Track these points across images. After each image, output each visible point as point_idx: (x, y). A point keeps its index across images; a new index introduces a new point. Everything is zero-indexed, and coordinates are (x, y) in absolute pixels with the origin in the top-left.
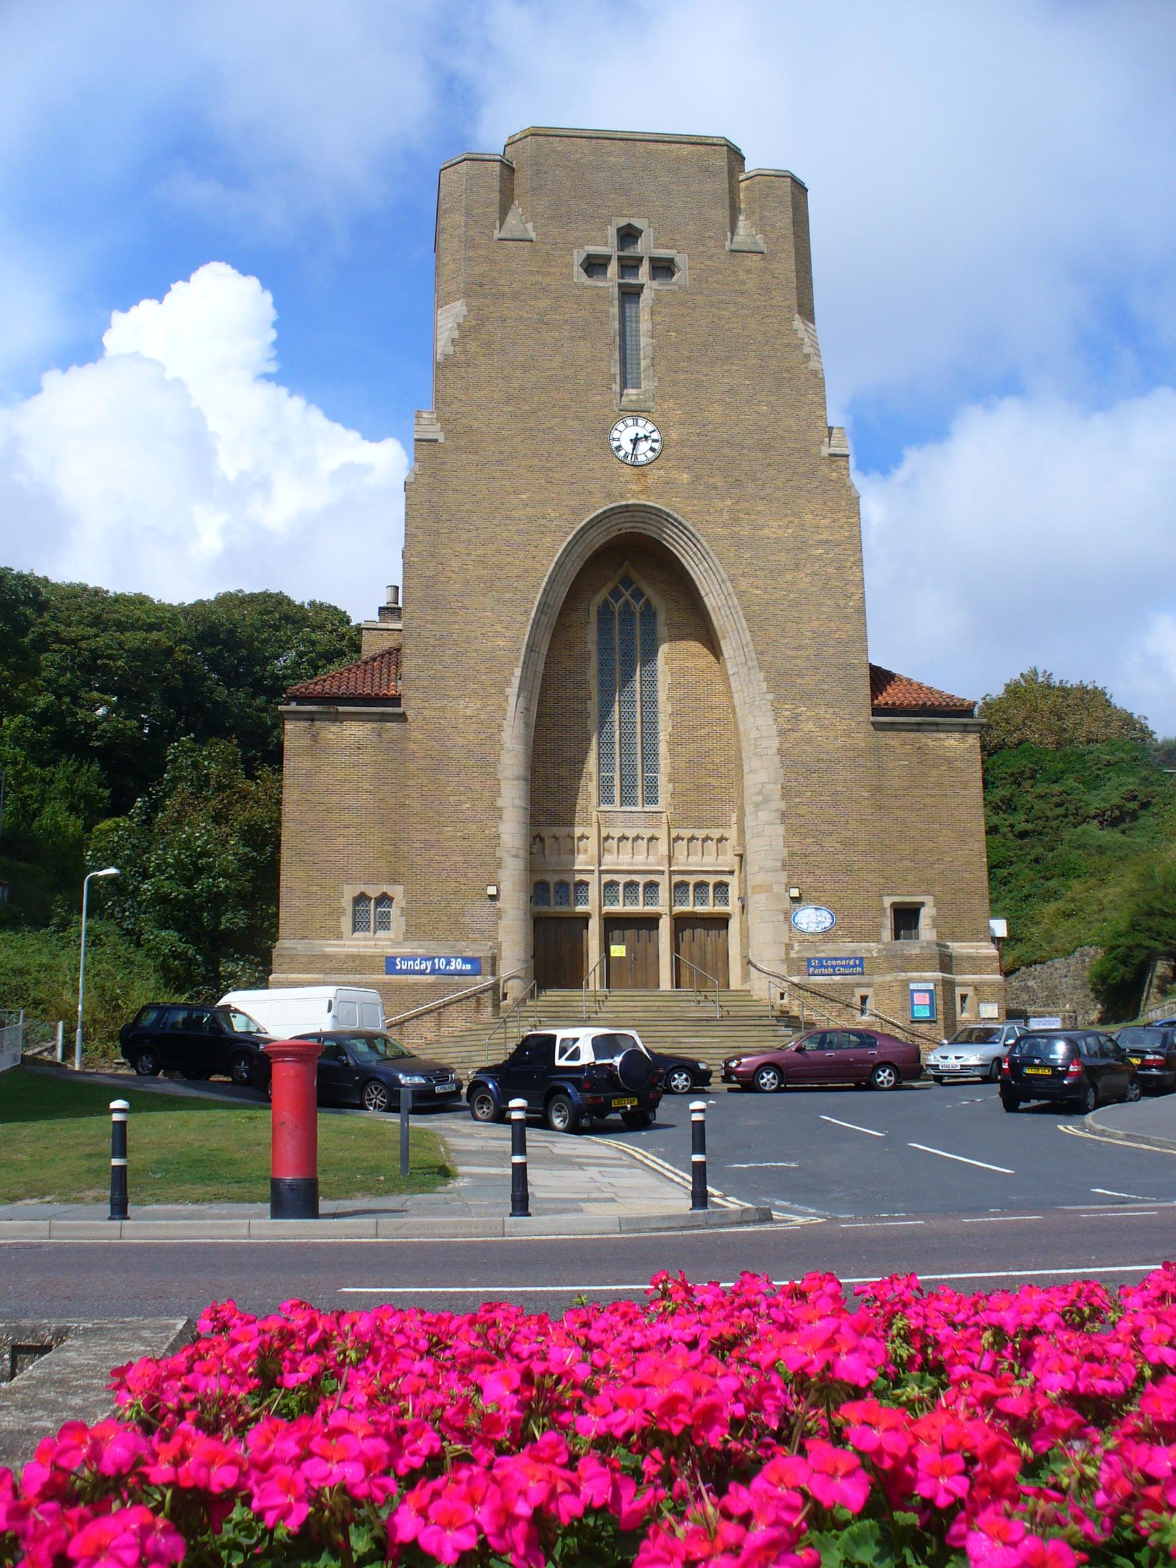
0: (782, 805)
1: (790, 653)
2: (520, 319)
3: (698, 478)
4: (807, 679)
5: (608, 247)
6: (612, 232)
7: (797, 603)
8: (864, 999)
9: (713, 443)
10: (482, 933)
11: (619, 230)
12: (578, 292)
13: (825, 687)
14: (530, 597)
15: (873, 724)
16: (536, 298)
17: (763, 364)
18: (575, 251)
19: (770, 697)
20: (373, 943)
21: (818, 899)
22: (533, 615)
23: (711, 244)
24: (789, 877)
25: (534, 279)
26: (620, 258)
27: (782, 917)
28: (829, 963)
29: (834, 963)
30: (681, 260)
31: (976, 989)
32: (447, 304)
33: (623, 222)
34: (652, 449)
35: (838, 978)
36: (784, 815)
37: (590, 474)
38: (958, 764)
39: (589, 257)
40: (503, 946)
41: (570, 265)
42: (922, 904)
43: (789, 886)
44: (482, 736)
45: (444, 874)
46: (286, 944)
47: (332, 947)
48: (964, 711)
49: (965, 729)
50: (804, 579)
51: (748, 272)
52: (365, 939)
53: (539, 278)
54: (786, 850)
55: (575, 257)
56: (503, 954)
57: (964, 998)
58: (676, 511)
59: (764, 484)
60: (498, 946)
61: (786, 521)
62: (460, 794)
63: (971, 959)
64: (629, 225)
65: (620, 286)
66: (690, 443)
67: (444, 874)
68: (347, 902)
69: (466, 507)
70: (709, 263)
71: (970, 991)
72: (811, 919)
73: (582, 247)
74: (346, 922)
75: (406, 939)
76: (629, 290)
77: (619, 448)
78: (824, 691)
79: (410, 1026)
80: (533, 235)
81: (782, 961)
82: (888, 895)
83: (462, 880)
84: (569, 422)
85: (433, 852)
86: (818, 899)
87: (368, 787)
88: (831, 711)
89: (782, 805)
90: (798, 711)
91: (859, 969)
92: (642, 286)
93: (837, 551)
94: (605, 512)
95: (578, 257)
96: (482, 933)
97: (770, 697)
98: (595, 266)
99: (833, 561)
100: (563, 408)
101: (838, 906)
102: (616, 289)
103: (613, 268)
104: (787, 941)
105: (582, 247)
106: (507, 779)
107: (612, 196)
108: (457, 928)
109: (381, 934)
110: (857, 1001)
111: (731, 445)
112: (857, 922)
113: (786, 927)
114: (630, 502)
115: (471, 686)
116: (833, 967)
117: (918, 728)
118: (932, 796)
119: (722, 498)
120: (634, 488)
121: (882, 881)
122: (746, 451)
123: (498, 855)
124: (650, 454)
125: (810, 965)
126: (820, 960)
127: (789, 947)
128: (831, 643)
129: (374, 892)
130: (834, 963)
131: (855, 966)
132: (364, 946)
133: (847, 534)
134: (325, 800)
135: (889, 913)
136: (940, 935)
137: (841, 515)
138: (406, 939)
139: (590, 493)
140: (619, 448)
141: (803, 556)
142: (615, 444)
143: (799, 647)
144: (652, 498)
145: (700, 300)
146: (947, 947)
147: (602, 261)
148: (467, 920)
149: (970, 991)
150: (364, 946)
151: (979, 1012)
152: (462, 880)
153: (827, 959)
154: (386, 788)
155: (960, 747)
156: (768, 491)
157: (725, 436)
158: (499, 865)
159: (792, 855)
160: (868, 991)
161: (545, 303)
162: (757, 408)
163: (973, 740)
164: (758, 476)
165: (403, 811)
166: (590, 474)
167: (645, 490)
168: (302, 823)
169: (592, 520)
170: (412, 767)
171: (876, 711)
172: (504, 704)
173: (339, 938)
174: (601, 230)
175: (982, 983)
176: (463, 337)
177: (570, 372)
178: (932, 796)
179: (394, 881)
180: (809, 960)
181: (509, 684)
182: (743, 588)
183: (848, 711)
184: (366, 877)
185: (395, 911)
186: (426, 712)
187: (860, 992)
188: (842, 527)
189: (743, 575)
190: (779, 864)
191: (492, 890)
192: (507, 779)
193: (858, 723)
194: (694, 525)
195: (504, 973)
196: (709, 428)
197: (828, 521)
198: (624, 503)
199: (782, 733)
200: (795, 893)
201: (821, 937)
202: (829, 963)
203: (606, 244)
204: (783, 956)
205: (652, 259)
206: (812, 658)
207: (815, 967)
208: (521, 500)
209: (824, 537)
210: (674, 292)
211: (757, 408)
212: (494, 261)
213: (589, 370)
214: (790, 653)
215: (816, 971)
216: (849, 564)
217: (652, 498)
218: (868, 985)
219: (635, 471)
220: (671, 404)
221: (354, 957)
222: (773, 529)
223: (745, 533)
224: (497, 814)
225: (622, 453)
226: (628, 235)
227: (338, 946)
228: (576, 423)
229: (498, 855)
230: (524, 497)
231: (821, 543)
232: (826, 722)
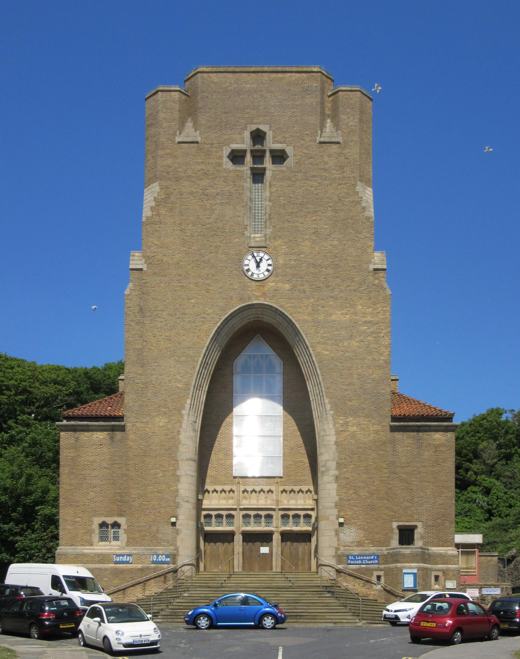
0: (336, 473)
1: (345, 387)
2: (192, 193)
3: (294, 287)
4: (354, 402)
5: (245, 143)
6: (247, 135)
7: (350, 358)
8: (379, 577)
9: (304, 265)
10: (168, 542)
11: (251, 133)
12: (226, 175)
13: (365, 406)
14: (196, 359)
15: (391, 427)
16: (201, 180)
17: (337, 215)
18: (224, 148)
19: (332, 412)
20: (110, 547)
21: (355, 523)
22: (197, 369)
23: (308, 139)
24: (339, 511)
25: (199, 167)
26: (252, 151)
27: (334, 533)
28: (359, 558)
29: (362, 558)
30: (289, 151)
31: (444, 573)
32: (149, 185)
33: (254, 127)
34: (268, 270)
35: (362, 566)
36: (337, 478)
37: (232, 287)
38: (441, 448)
39: (233, 151)
40: (180, 549)
41: (220, 158)
42: (416, 527)
43: (338, 517)
44: (168, 437)
45: (148, 511)
46: (61, 549)
47: (87, 550)
48: (449, 418)
49: (446, 429)
50: (354, 344)
51: (330, 156)
52: (105, 545)
53: (203, 167)
54: (337, 497)
55: (224, 151)
56: (180, 553)
57: (437, 578)
58: (281, 307)
59: (334, 288)
60: (177, 549)
61: (345, 311)
62: (157, 469)
63: (441, 555)
64: (258, 130)
65: (252, 169)
66: (290, 266)
67: (148, 511)
68: (95, 526)
69: (160, 308)
70: (306, 151)
71: (440, 574)
72: (350, 535)
73: (228, 145)
74: (96, 537)
75: (127, 545)
76: (256, 172)
77: (248, 270)
78: (364, 409)
79: (129, 591)
80: (199, 139)
81: (334, 557)
82: (396, 521)
83: (158, 514)
84: (219, 256)
85: (141, 500)
86: (355, 523)
87: (106, 465)
88: (367, 419)
89: (336, 473)
90: (348, 420)
91: (376, 561)
92: (265, 169)
93: (375, 327)
94: (239, 309)
95: (226, 151)
96: (168, 542)
97: (332, 412)
98: (237, 157)
99: (372, 333)
100: (216, 247)
101: (366, 527)
102: (249, 172)
103: (248, 158)
104: (336, 546)
105: (228, 145)
106: (183, 460)
107: (247, 111)
108: (155, 540)
109: (114, 543)
110: (374, 579)
111: (314, 266)
112: (377, 536)
113: (336, 539)
114: (254, 302)
115: (163, 409)
116: (362, 560)
117: (418, 429)
118: (424, 467)
119: (308, 298)
120: (257, 294)
121: (392, 513)
122: (324, 269)
123: (177, 501)
124: (266, 273)
125: (348, 559)
126: (354, 556)
127: (337, 549)
128: (369, 381)
129: (110, 520)
130: (362, 558)
131: (374, 559)
132: (104, 549)
133: (382, 317)
134: (83, 472)
135: (397, 531)
136: (425, 543)
137: (379, 306)
138: (127, 545)
139: (231, 298)
140: (248, 270)
141: (355, 331)
142: (246, 268)
143: (350, 384)
144: (267, 300)
145: (299, 175)
146: (428, 550)
147: (241, 154)
148: (160, 536)
149: (440, 574)
150: (104, 549)
151: (445, 585)
152: (158, 514)
153: (358, 556)
154: (116, 466)
155: (444, 440)
156: (336, 293)
157: (312, 261)
158: (177, 506)
159: (341, 499)
160: (381, 573)
161: (205, 183)
162: (331, 243)
163: (451, 436)
164: (330, 284)
165: (125, 478)
166: (232, 287)
167: (264, 295)
168: (70, 485)
169: (232, 314)
170: (131, 454)
171: (394, 419)
172: (181, 419)
173: (92, 545)
174: (240, 133)
175: (448, 570)
176: (158, 206)
177: (220, 225)
178: (424, 467)
179: (120, 515)
180: (348, 556)
181: (183, 408)
182: (319, 351)
183: (377, 419)
184: (105, 513)
185: (121, 531)
186: (137, 424)
187: (376, 573)
188: (379, 313)
189: (318, 343)
190: (333, 505)
191: (173, 520)
192: (183, 460)
193: (383, 426)
194: (291, 314)
195: (180, 563)
196: (302, 256)
197: (370, 309)
198: (250, 303)
199: (338, 433)
200: (341, 520)
201: (356, 544)
202: (359, 558)
203: (243, 143)
204: (334, 554)
205: (271, 151)
206: (358, 390)
207: (351, 560)
208: (191, 303)
209: (369, 318)
210: (283, 172)
211: (331, 243)
212: (176, 157)
213: (232, 223)
214: (345, 387)
215: (352, 562)
216: (382, 335)
217: (267, 300)
218: (381, 570)
219: (258, 283)
220: (280, 242)
221: (99, 555)
222: (338, 316)
223: (321, 317)
224: (177, 479)
225: (250, 273)
226: (258, 136)
227: (90, 549)
228: (223, 256)
229: (177, 501)
230: (193, 301)
231: (365, 322)
232: (364, 426)
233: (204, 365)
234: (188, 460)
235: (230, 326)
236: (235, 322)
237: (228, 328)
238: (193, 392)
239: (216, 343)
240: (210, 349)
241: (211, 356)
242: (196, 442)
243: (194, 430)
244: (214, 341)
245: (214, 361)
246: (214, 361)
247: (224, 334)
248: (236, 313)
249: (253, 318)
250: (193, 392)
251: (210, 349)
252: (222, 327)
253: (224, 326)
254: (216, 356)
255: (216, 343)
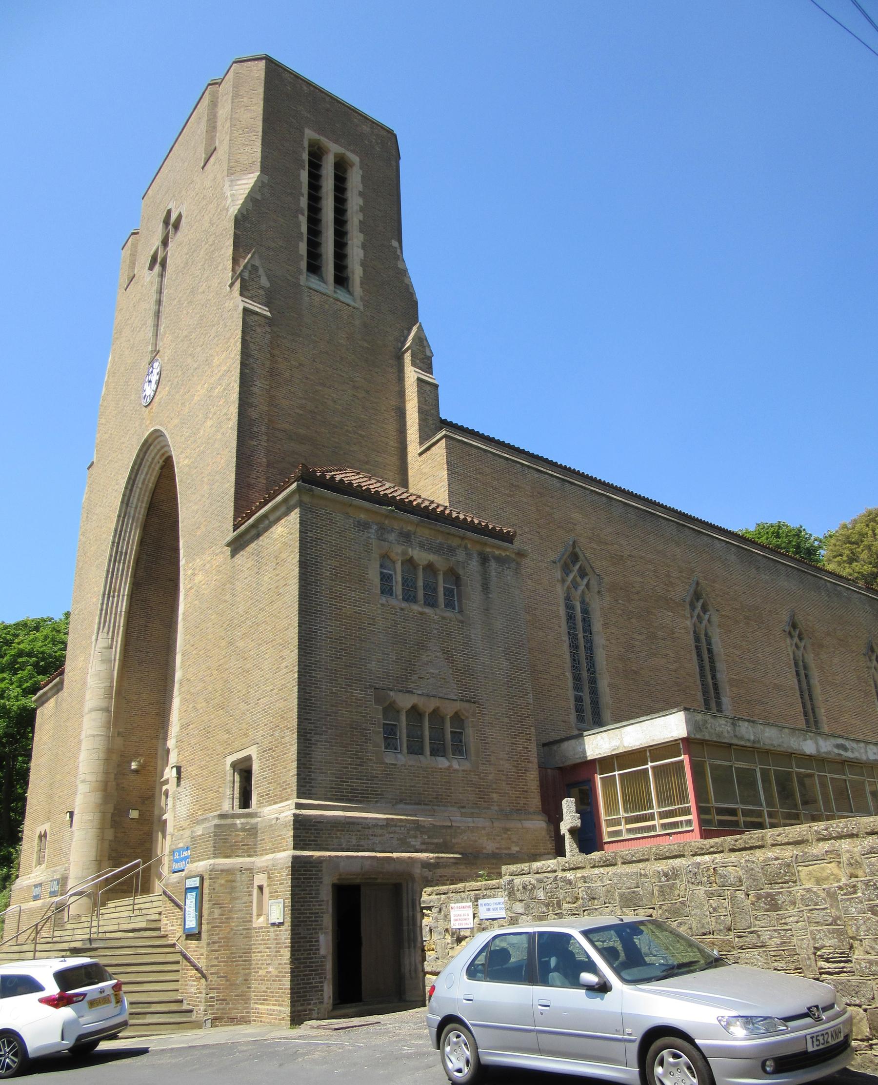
233: (116, 557)
234: (91, 710)
235: (140, 485)
236: (143, 476)
237: (138, 490)
238: (102, 604)
239: (128, 519)
240: (121, 531)
241: (124, 540)
242: (113, 678)
243: (108, 661)
244: (124, 518)
245: (132, 546)
246: (132, 546)
247: (135, 501)
248: (138, 462)
249: (161, 458)
250: (102, 604)
251: (121, 531)
252: (128, 492)
253: (131, 490)
254: (135, 535)
255: (128, 519)
